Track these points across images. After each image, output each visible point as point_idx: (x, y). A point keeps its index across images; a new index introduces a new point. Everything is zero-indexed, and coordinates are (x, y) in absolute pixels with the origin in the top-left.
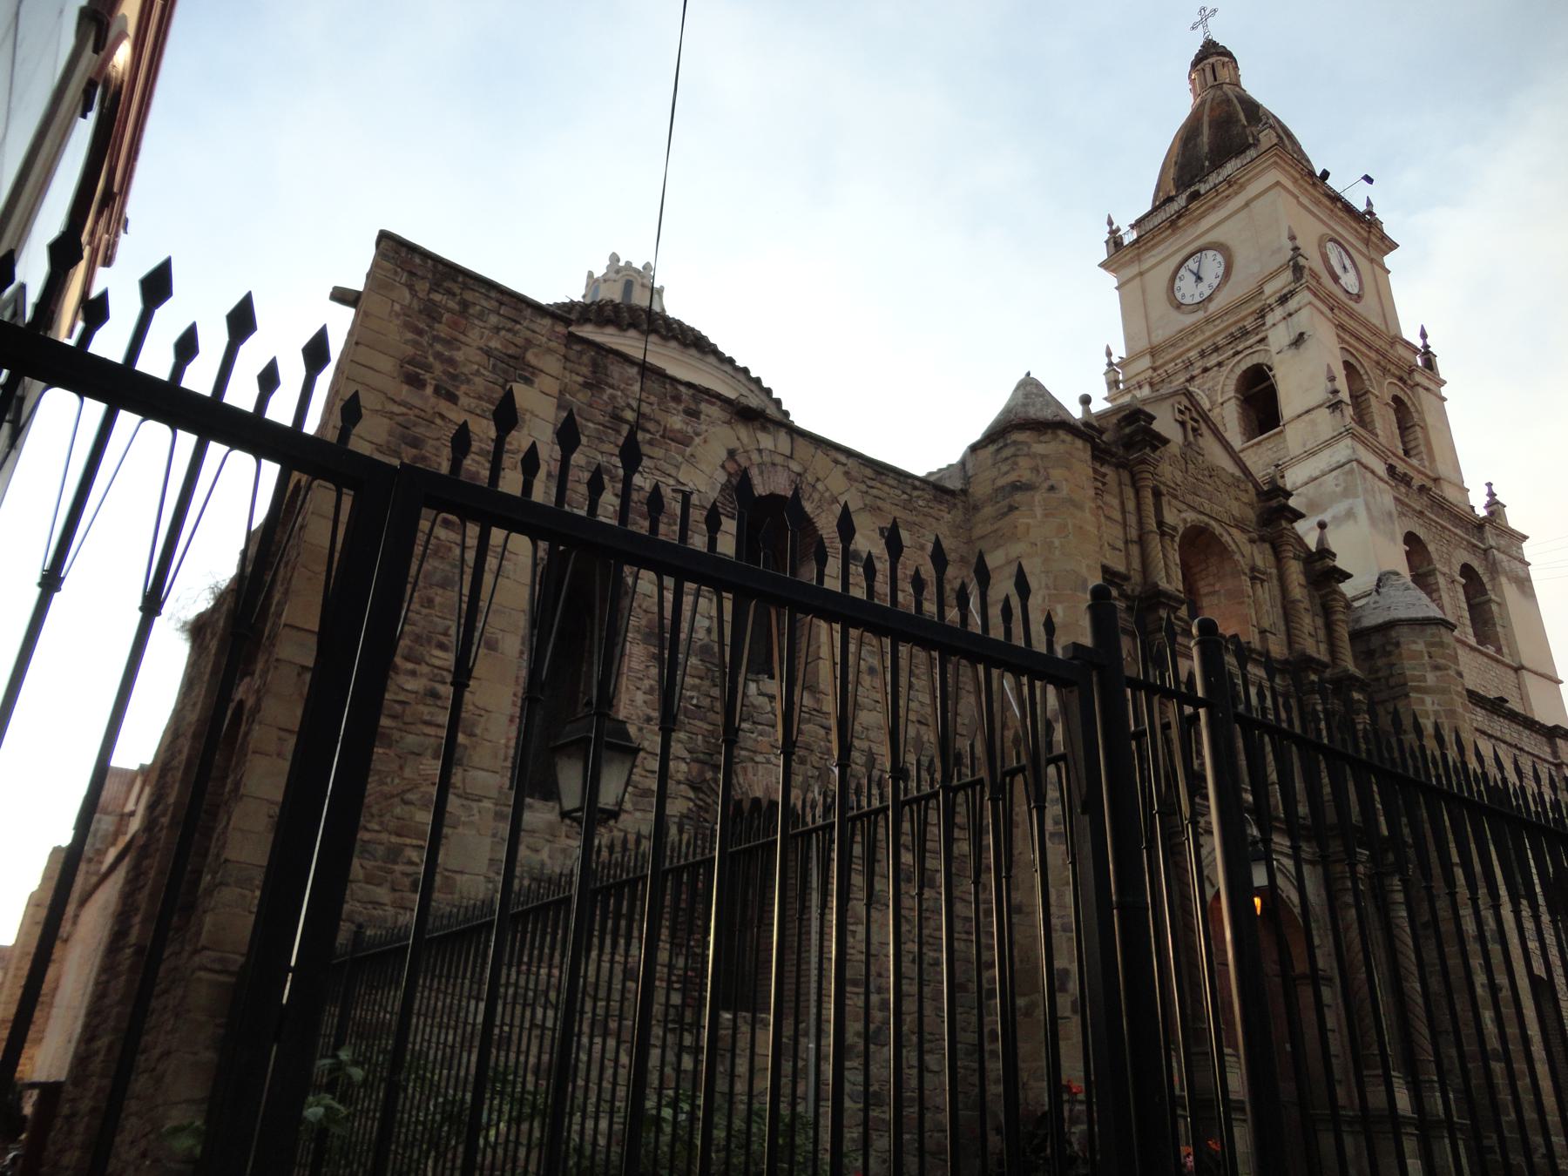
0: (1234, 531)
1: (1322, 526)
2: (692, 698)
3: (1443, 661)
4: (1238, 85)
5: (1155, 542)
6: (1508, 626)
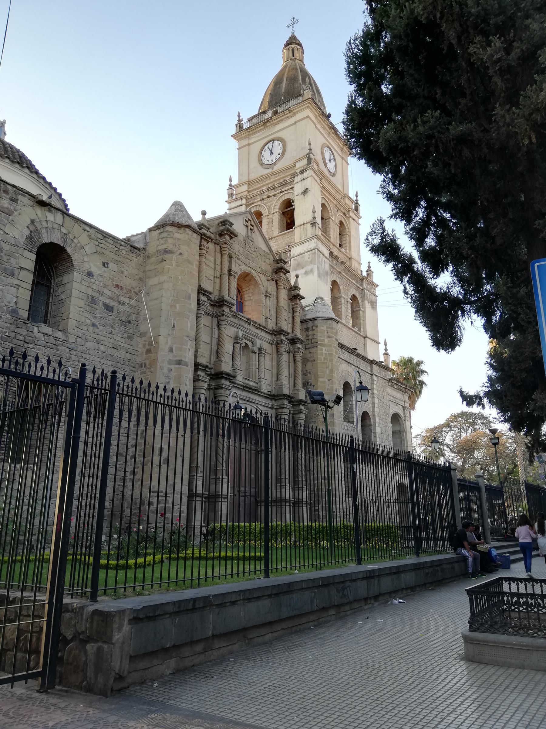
0: (261, 276)
1: (297, 276)
2: (6, 332)
4: (302, 61)
5: (226, 277)
6: (364, 321)
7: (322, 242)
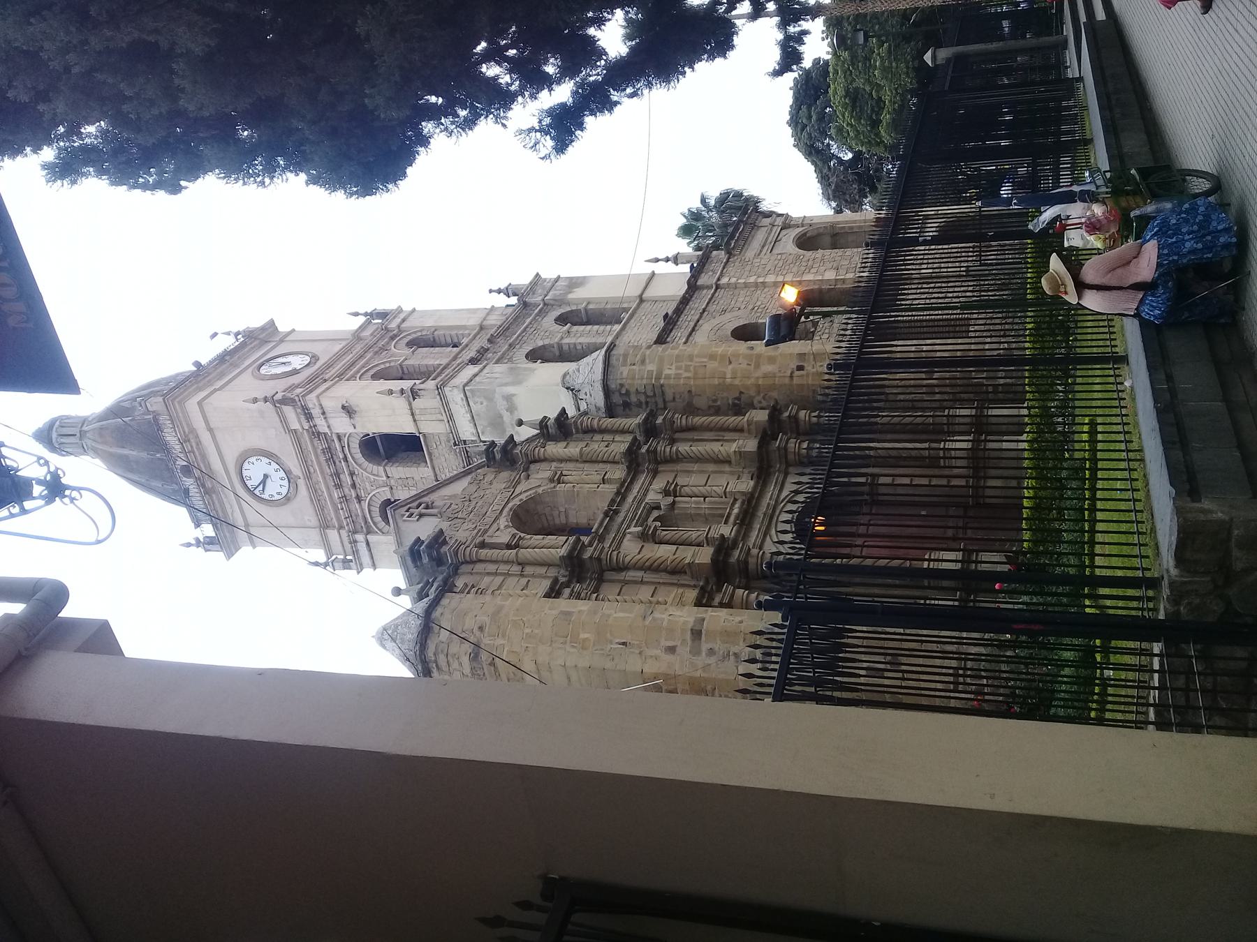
0: (518, 491)
1: (520, 423)
5: (524, 553)
7: (452, 377)
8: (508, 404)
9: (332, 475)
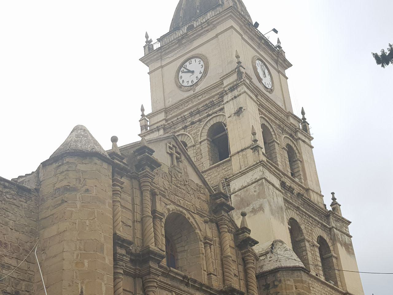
0: (197, 217)
1: (244, 214)
3: (302, 291)
7: (270, 171)
8: (257, 208)
9: (198, 109)
